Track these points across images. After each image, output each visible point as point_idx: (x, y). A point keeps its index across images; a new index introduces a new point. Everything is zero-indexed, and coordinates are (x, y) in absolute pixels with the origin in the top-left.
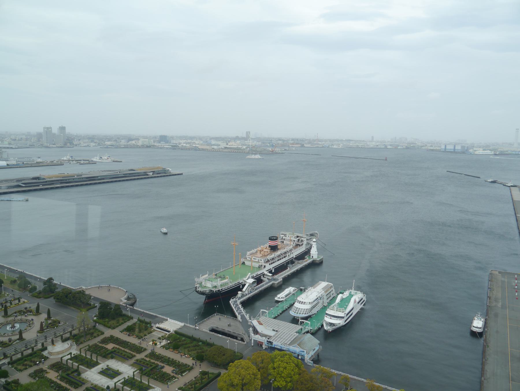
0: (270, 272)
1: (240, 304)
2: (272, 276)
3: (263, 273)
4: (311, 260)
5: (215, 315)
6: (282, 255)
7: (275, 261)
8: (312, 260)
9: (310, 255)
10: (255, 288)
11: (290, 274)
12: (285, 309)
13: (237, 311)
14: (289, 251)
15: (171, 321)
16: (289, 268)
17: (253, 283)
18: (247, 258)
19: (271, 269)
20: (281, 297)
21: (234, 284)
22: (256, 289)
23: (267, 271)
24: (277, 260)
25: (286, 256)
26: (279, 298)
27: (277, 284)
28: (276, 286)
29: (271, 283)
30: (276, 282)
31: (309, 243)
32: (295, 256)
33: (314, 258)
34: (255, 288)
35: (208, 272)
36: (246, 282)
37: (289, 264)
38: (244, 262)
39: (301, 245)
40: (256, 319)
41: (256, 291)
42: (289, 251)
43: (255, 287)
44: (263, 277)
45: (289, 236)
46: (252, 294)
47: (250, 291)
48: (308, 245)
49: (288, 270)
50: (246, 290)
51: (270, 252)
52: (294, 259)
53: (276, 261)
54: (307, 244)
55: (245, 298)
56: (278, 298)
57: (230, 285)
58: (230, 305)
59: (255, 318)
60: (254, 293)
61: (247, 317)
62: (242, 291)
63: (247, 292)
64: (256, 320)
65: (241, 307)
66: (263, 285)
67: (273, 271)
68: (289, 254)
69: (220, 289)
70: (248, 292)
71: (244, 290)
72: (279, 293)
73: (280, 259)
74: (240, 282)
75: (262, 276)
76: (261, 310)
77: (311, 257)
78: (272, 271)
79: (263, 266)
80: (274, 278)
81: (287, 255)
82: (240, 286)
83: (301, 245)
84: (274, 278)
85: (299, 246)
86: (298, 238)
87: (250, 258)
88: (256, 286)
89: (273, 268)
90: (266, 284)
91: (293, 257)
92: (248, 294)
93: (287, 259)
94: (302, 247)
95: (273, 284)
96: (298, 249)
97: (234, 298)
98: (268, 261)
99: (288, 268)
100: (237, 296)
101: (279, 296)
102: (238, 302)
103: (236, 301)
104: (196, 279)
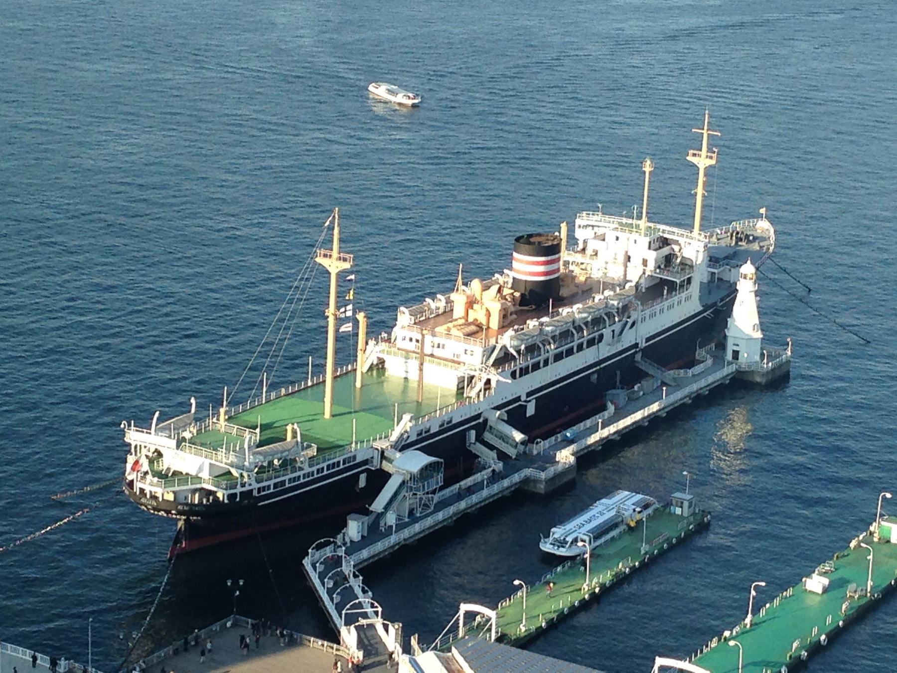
0: (516, 417)
1: (355, 576)
2: (523, 443)
3: (478, 416)
4: (727, 370)
5: (229, 624)
6: (579, 329)
7: (541, 358)
8: (733, 368)
9: (722, 346)
10: (436, 498)
11: (616, 437)
12: (587, 596)
13: (339, 608)
14: (614, 311)
15: (15, 650)
16: (611, 408)
17: (427, 471)
18: (400, 344)
19: (518, 399)
20: (569, 539)
21: (325, 465)
22: (442, 505)
23: (498, 408)
24: (551, 355)
25: (601, 337)
26: (562, 543)
27: (550, 481)
28: (541, 488)
29: (516, 478)
30: (543, 475)
31: (720, 279)
32: (648, 340)
33: (744, 356)
34: (436, 498)
35: (193, 401)
36: (390, 461)
37: (614, 387)
38: (382, 362)
39: (682, 286)
40: (435, 648)
41: (440, 516)
42: (614, 311)
43: (434, 492)
44: (480, 439)
45: (617, 238)
46: (417, 527)
47: (411, 512)
48: (718, 287)
49: (606, 414)
50: (387, 507)
51: (516, 313)
52: (638, 357)
53: (546, 363)
54: (711, 281)
55: (379, 547)
56: (556, 540)
57: (307, 470)
58: (303, 576)
59: (429, 644)
60: (429, 522)
61: (390, 639)
62: (367, 512)
63: (391, 519)
64: (432, 652)
65: (358, 591)
66: (477, 488)
67: (531, 410)
68: (617, 327)
69: (256, 486)
70: (399, 518)
71: (378, 505)
72: (562, 520)
73: (570, 352)
74: (358, 460)
75: (473, 433)
76: (464, 607)
77: (729, 356)
78: (523, 408)
79: (480, 385)
80: (535, 452)
81: (607, 332)
82: (356, 476)
83: (682, 286)
84: (535, 452)
85: (670, 292)
86: (666, 251)
87: (411, 340)
88: (441, 488)
89: (529, 394)
90: (495, 477)
91: (636, 345)
92: (400, 527)
93: (604, 350)
94: (684, 295)
95: (526, 481)
96: (666, 303)
97: (327, 544)
98: (505, 358)
99: (609, 404)
100: (340, 536)
101: (557, 532)
102: (347, 568)
103: (337, 561)
104: (133, 436)
